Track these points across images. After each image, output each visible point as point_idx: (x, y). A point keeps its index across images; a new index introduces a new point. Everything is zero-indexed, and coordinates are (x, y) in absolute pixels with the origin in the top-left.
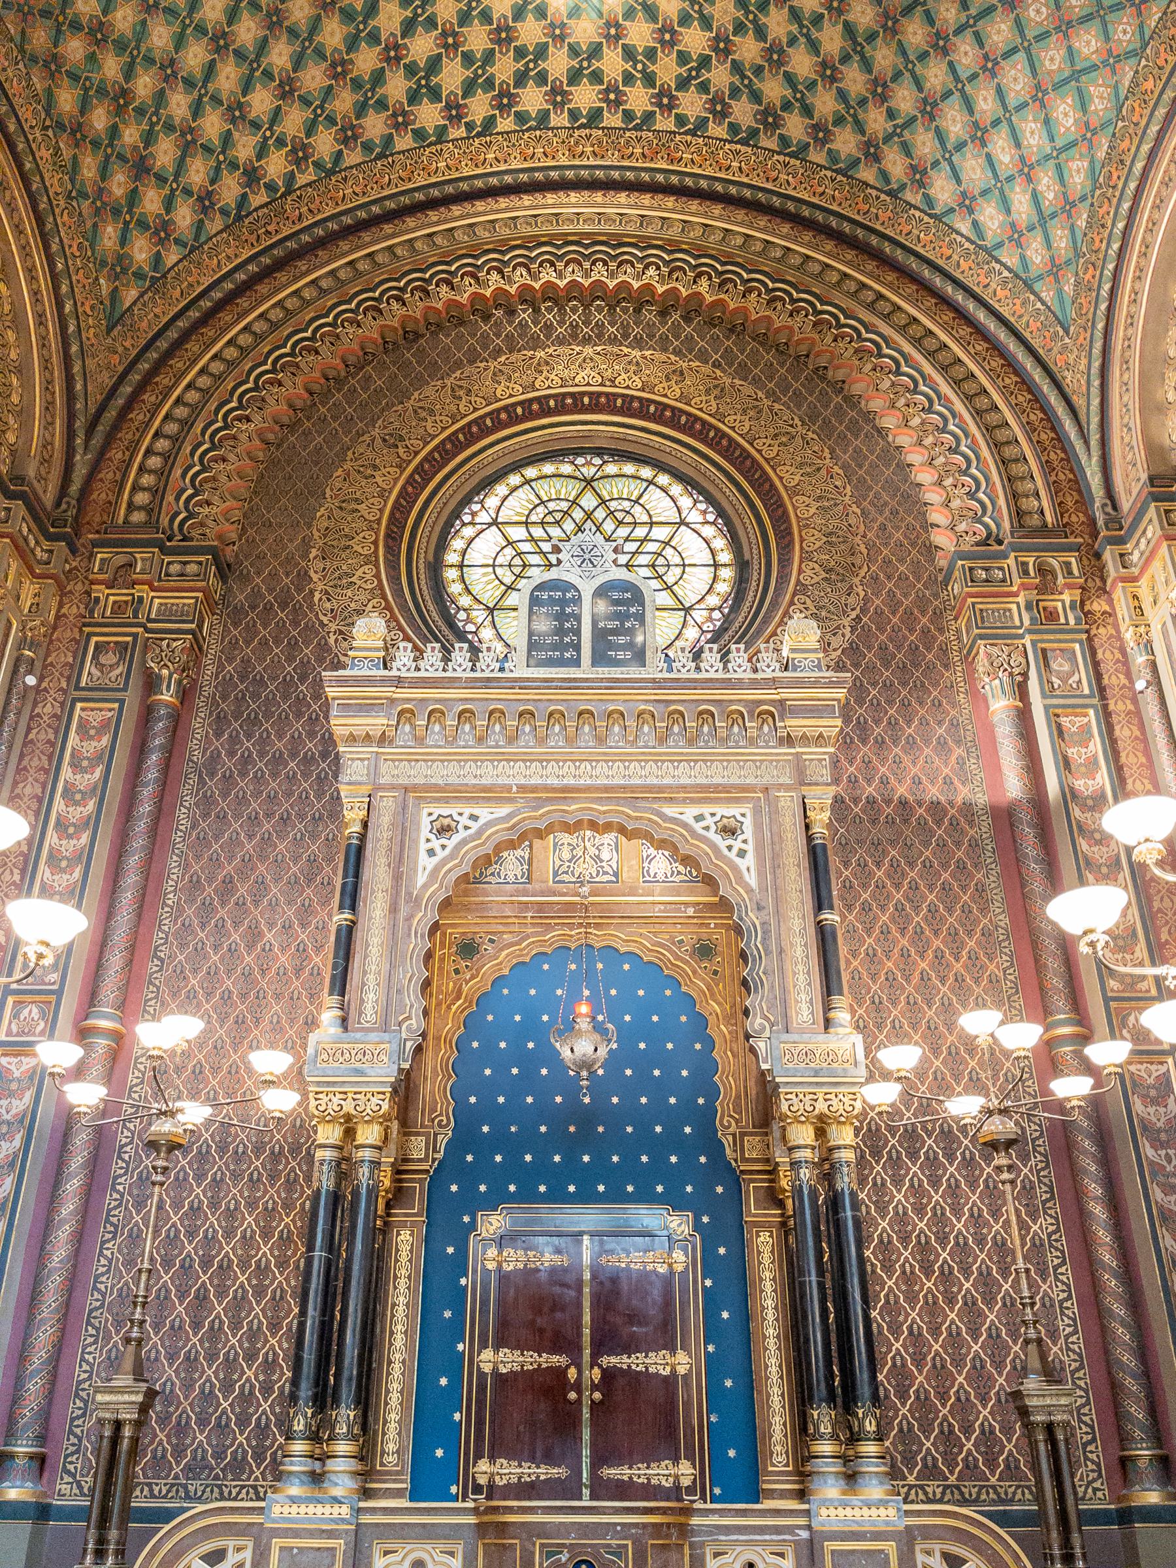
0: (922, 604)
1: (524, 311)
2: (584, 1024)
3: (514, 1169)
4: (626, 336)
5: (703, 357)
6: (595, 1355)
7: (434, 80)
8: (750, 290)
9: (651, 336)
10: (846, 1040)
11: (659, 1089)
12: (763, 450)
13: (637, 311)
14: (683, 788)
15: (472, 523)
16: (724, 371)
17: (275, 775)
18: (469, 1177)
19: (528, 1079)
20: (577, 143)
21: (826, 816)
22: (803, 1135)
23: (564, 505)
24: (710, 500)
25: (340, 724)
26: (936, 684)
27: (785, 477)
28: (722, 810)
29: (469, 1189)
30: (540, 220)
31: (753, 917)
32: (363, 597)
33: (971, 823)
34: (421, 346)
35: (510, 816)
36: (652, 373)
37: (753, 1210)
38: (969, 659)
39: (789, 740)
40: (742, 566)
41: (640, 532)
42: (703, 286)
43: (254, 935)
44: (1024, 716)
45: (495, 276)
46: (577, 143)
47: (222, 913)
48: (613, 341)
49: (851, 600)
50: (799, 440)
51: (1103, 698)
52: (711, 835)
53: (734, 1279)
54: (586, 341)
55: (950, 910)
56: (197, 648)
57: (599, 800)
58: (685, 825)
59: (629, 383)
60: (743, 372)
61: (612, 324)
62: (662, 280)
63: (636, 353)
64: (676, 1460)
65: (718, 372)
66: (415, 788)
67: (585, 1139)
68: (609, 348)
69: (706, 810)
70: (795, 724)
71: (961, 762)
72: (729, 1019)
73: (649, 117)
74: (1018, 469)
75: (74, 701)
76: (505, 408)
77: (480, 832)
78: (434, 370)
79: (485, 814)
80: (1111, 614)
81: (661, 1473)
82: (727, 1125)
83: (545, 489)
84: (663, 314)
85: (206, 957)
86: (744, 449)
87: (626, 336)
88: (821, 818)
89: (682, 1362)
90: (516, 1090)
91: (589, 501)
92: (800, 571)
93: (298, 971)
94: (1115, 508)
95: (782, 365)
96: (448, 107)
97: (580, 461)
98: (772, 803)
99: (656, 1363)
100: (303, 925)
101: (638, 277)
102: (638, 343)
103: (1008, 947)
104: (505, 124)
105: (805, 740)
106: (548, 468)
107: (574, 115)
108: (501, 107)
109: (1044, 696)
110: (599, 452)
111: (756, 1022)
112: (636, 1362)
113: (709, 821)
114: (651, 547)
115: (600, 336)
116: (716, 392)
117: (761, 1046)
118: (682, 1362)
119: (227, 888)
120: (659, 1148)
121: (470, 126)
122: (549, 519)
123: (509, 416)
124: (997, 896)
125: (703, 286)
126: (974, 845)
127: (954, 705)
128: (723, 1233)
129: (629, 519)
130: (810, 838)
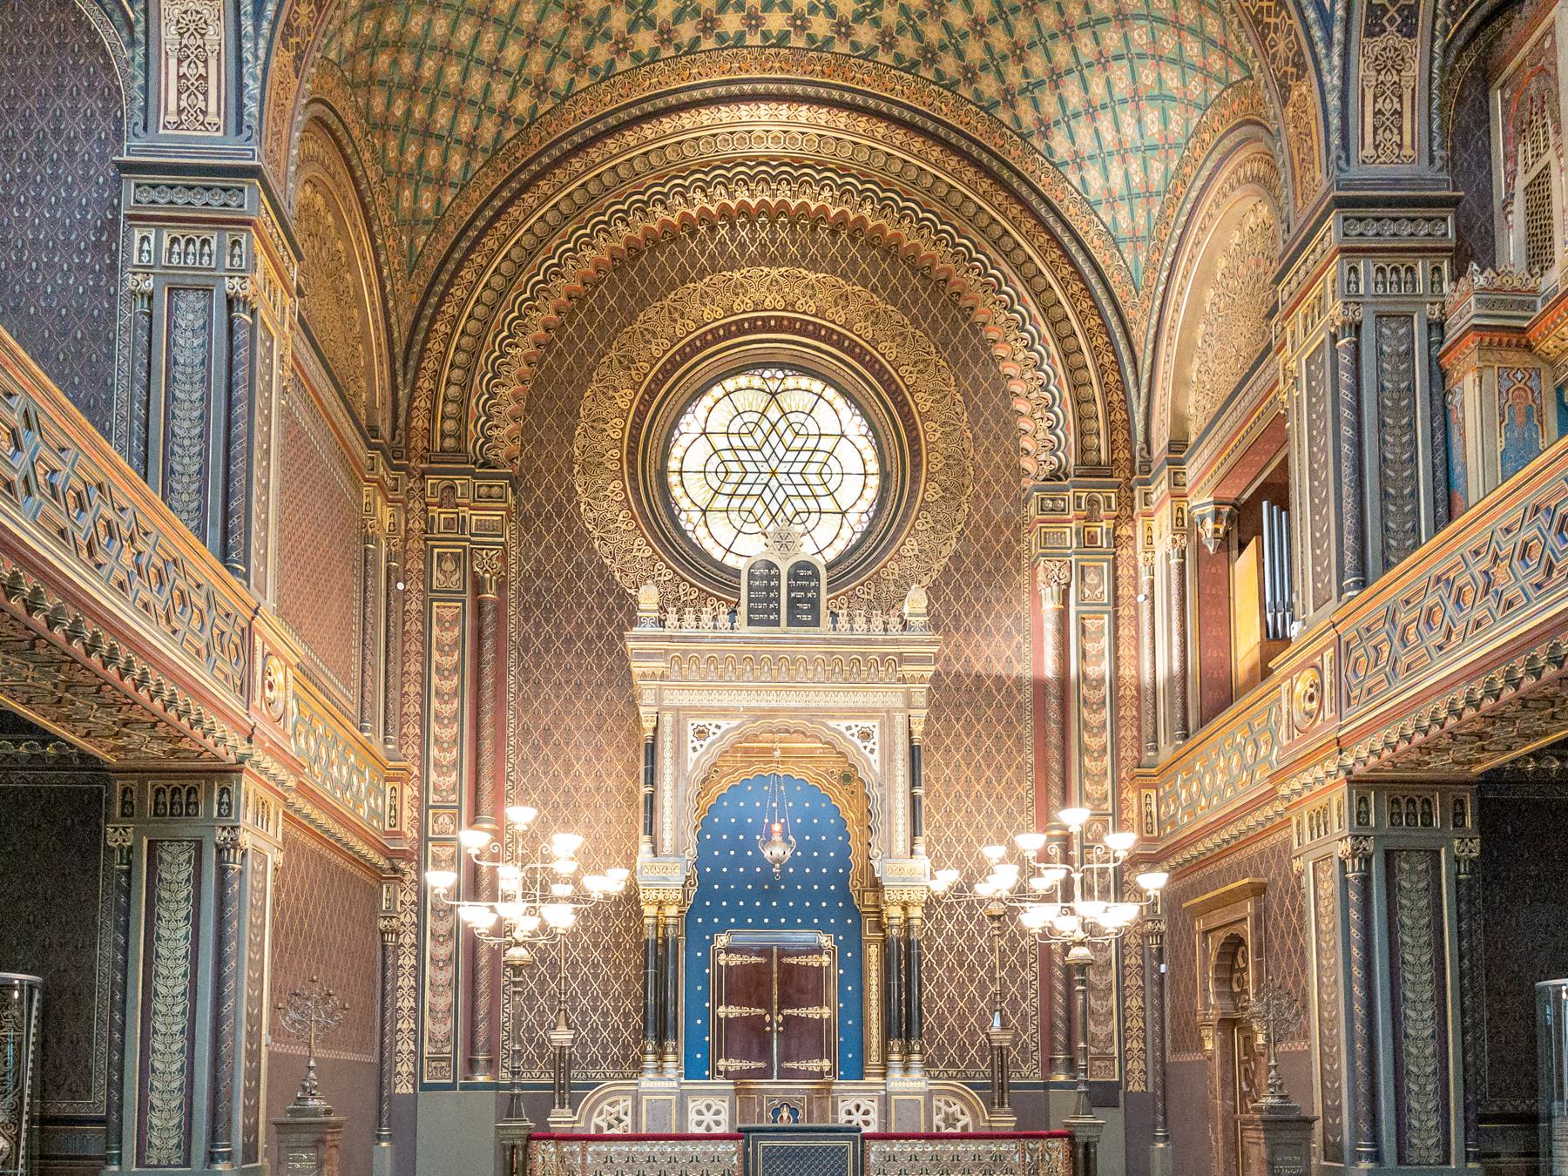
0: (1007, 519)
1: (723, 227)
2: (777, 838)
3: (733, 910)
4: (804, 256)
6: (780, 1009)
7: (650, 12)
8: (904, 217)
9: (824, 257)
10: (922, 863)
11: (816, 865)
13: (814, 229)
14: (841, 709)
18: (708, 914)
19: (741, 858)
20: (767, 60)
21: (921, 728)
22: (896, 912)
23: (755, 417)
24: (864, 414)
25: (637, 667)
26: (1009, 586)
27: (921, 402)
28: (862, 723)
29: (708, 921)
30: (736, 137)
31: (875, 792)
32: (616, 508)
33: (1019, 691)
34: (644, 270)
35: (739, 727)
36: (824, 297)
37: (868, 934)
38: (1034, 566)
39: (903, 680)
40: (885, 475)
45: (699, 195)
46: (767, 60)
47: (546, 751)
48: (793, 262)
49: (959, 516)
50: (932, 367)
51: (1116, 605)
52: (855, 739)
53: (857, 971)
54: (773, 262)
55: (999, 751)
57: (791, 717)
58: (840, 733)
59: (806, 309)
60: (893, 298)
62: (834, 203)
63: (812, 276)
64: (821, 1059)
66: (684, 708)
67: (774, 892)
69: (852, 723)
70: (908, 669)
72: (860, 822)
73: (828, 41)
75: (432, 600)
77: (722, 737)
78: (656, 294)
79: (725, 725)
81: (814, 1065)
82: (854, 885)
85: (540, 780)
86: (891, 376)
87: (804, 256)
88: (918, 729)
89: (826, 1012)
90: (734, 863)
91: (774, 413)
92: (925, 490)
93: (598, 789)
96: (661, 32)
97: (767, 374)
98: (891, 719)
99: (813, 1012)
102: (814, 266)
103: (1032, 776)
104: (708, 44)
105: (913, 680)
107: (765, 36)
108: (705, 30)
109: (1077, 604)
110: (781, 366)
111: (874, 851)
112: (802, 1012)
113: (854, 730)
115: (783, 255)
116: (872, 318)
117: (876, 864)
118: (826, 1012)
120: (816, 898)
121: (678, 47)
122: (744, 430)
124: (1029, 742)
126: (1020, 706)
127: (1019, 601)
128: (852, 944)
130: (911, 741)
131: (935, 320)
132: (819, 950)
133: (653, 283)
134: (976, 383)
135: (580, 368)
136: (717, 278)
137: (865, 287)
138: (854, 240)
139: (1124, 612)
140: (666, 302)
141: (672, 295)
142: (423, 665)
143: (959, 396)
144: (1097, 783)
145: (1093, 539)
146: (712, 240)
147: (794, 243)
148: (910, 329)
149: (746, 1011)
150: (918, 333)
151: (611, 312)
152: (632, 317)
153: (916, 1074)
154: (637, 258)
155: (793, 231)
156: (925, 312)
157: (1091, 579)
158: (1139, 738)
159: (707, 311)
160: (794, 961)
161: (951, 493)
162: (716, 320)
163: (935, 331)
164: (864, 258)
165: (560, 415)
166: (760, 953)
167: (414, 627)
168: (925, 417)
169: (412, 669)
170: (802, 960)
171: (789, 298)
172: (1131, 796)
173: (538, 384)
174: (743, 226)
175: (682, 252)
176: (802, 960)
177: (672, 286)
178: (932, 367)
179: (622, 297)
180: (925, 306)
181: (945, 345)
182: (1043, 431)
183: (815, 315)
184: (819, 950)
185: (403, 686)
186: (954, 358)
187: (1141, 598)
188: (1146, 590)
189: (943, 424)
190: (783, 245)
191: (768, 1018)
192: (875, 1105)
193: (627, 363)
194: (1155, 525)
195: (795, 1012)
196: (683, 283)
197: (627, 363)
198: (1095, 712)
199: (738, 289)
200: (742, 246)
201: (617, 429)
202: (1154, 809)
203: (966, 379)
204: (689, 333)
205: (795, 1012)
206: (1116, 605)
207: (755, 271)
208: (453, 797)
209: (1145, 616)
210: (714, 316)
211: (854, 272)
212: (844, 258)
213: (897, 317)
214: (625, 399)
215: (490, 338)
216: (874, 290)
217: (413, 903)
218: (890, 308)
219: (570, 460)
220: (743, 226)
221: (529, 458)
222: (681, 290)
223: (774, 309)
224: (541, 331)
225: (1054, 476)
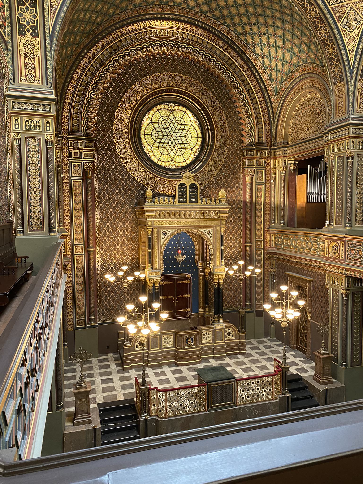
4: (182, 70)
5: (199, 79)
9: (187, 71)
12: (210, 110)
16: (203, 84)
17: (114, 193)
42: (201, 58)
43: (115, 228)
44: (252, 184)
48: (178, 72)
54: (173, 71)
59: (182, 87)
71: (239, 192)
74: (260, 130)
80: (270, 163)
83: (163, 113)
87: (182, 70)
94: (276, 140)
100: (124, 226)
102: (184, 74)
106: (162, 106)
114: (185, 131)
115: (176, 69)
119: (108, 219)
131: (219, 93)
132: (187, 279)
133: (136, 76)
134: (229, 114)
135: (115, 102)
136: (156, 75)
137: (199, 81)
139: (268, 184)
142: (70, 200)
144: (259, 232)
145: (260, 163)
146: (155, 62)
149: (167, 297)
150: (214, 97)
151: (124, 84)
153: (221, 324)
154: (131, 66)
155: (178, 61)
157: (260, 175)
158: (270, 219)
159: (153, 86)
160: (181, 282)
161: (223, 146)
162: (156, 89)
163: (219, 97)
165: (108, 117)
166: (170, 280)
167: (66, 188)
169: (67, 201)
170: (183, 282)
173: (101, 107)
174: (164, 58)
175: (145, 66)
176: (183, 282)
177: (143, 77)
179: (127, 80)
180: (216, 88)
182: (249, 131)
183: (185, 89)
184: (187, 279)
185: (64, 206)
187: (272, 181)
188: (273, 178)
190: (176, 65)
191: (173, 298)
192: (211, 332)
193: (129, 101)
194: (277, 161)
195: (181, 296)
198: (259, 212)
200: (163, 65)
201: (126, 122)
202: (274, 239)
204: (148, 93)
205: (181, 296)
206: (266, 182)
207: (167, 73)
208: (81, 241)
209: (273, 185)
212: (193, 72)
216: (202, 82)
217: (70, 274)
219: (112, 132)
221: (99, 131)
223: (173, 87)
225: (250, 145)
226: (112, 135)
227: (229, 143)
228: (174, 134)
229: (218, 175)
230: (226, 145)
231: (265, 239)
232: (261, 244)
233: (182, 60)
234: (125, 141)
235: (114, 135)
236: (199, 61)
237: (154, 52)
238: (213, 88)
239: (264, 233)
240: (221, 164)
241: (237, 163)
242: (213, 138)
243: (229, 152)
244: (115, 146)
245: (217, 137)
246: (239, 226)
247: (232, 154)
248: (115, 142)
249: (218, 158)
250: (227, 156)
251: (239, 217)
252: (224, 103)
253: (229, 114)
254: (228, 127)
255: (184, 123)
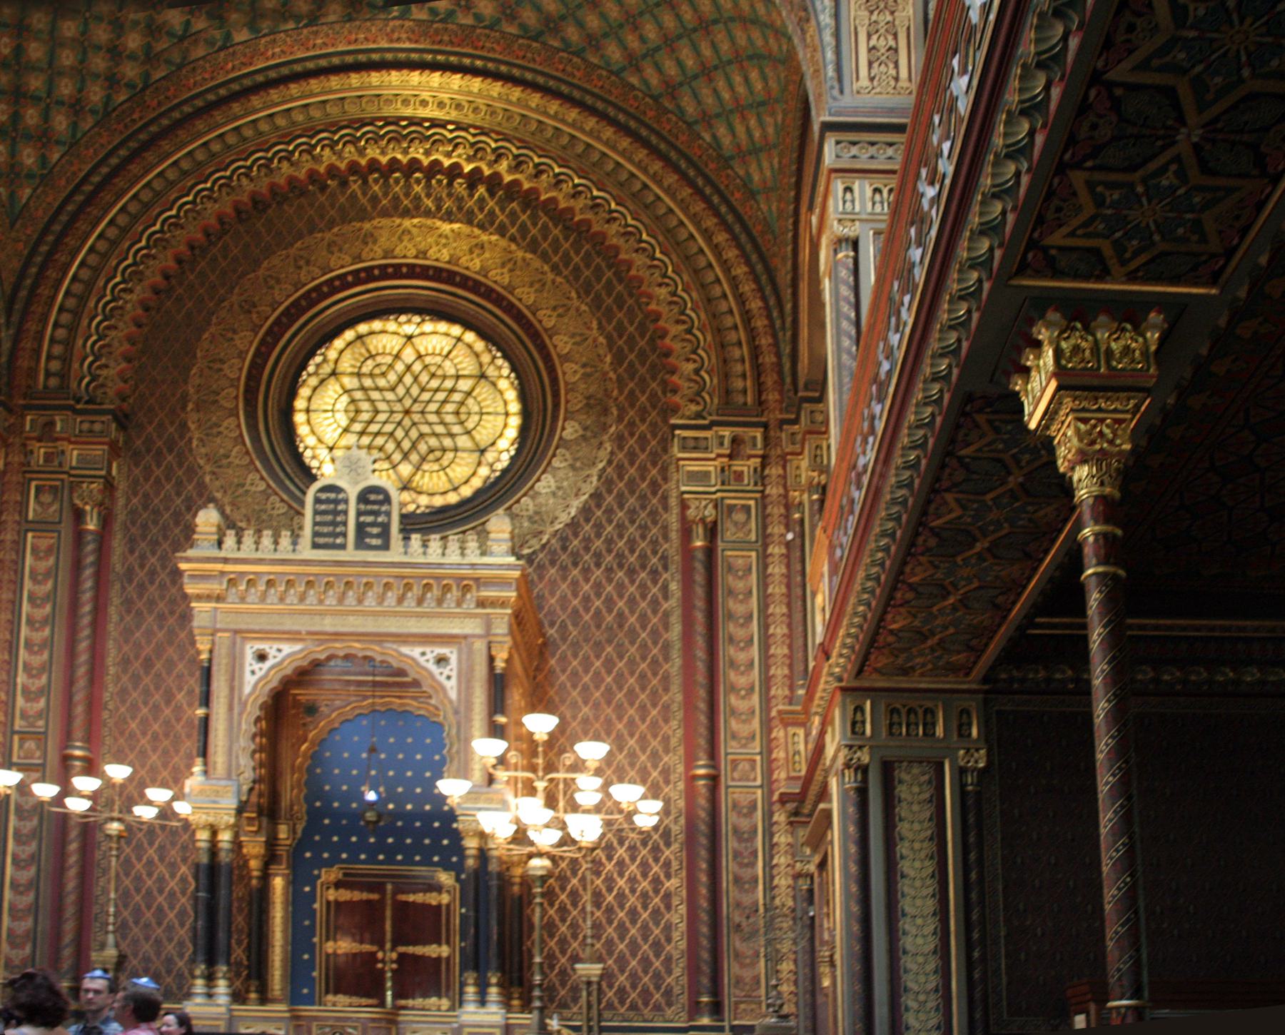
4: (439, 208)
5: (502, 231)
9: (460, 209)
15: (316, 373)
41: (449, 384)
48: (428, 214)
50: (572, 312)
54: (406, 213)
56: (109, 485)
60: (533, 247)
61: (428, 195)
65: (513, 247)
68: (423, 220)
76: (339, 277)
84: (472, 187)
87: (439, 208)
95: (567, 239)
101: (449, 155)
102: (449, 217)
116: (510, 266)
123: (343, 283)
125: (503, 166)
129: (440, 372)
134: (620, 329)
136: (347, 229)
137: (503, 236)
138: (492, 193)
140: (292, 251)
141: (298, 244)
143: (601, 340)
144: (744, 722)
147: (428, 195)
148: (550, 276)
150: (559, 279)
152: (257, 263)
154: (264, 210)
155: (428, 185)
156: (566, 259)
163: (577, 279)
164: (503, 210)
168: (566, 358)
171: (422, 246)
172: (778, 733)
174: (376, 181)
177: (300, 236)
178: (572, 312)
181: (588, 293)
186: (597, 304)
189: (584, 366)
196: (311, 232)
197: (249, 307)
198: (742, 649)
199: (369, 238)
203: (609, 322)
207: (385, 222)
210: (344, 266)
211: (492, 224)
212: (481, 209)
213: (537, 263)
214: (248, 343)
215: (101, 283)
216: (513, 239)
218: (529, 256)
220: (376, 181)
222: (308, 240)
224: (159, 278)
226: (184, 408)
227: (620, 419)
228: (417, 407)
229: (573, 525)
230: (605, 428)
231: (770, 751)
232: (753, 768)
233: (440, 182)
234: (225, 424)
235: (190, 406)
236: (496, 176)
237: (338, 163)
238: (556, 252)
239: (767, 726)
240: (588, 489)
241: (654, 486)
242: (556, 405)
243: (621, 448)
244: (190, 440)
245: (567, 402)
246: (666, 708)
247: (632, 456)
248: (192, 427)
249: (572, 467)
250: (610, 462)
251: (666, 679)
252: (598, 298)
253: (620, 329)
254: (615, 371)
255: (452, 372)
